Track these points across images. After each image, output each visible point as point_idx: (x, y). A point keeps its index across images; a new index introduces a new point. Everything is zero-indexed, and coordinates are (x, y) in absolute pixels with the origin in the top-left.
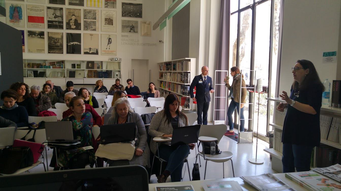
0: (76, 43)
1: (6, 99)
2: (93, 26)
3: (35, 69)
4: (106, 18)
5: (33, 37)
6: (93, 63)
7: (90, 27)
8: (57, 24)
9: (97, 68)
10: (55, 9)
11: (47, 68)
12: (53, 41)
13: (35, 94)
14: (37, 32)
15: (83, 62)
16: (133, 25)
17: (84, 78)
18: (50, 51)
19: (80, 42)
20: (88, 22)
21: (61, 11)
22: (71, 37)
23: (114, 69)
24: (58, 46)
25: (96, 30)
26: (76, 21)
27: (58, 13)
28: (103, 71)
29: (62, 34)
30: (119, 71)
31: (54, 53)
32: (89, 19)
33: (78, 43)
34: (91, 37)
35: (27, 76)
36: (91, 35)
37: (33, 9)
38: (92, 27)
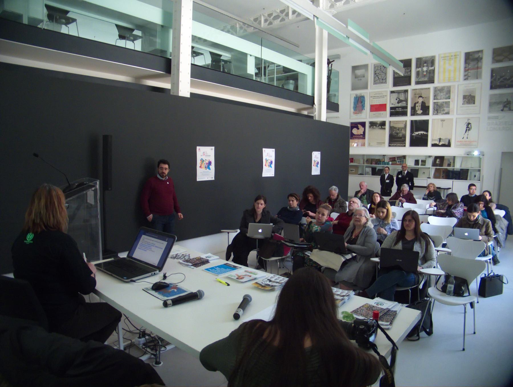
0: (422, 132)
1: (290, 198)
2: (445, 109)
3: (374, 165)
4: (464, 95)
5: (375, 128)
6: (442, 158)
7: (441, 110)
8: (400, 110)
9: (448, 166)
10: (399, 92)
11: (386, 165)
12: (395, 132)
13: (333, 195)
14: (378, 123)
15: (430, 157)
16: (508, 100)
17: (428, 178)
18: (391, 144)
19: (427, 131)
20: (439, 104)
21: (406, 94)
22: (418, 126)
23: (472, 167)
24: (401, 138)
25: (450, 113)
26: (423, 103)
27: (402, 97)
28: (455, 170)
29: (405, 122)
30: (479, 171)
31: (395, 146)
32: (440, 99)
33: (425, 133)
34: (443, 123)
35: (364, 174)
36: (443, 120)
37: (376, 96)
38: (444, 110)
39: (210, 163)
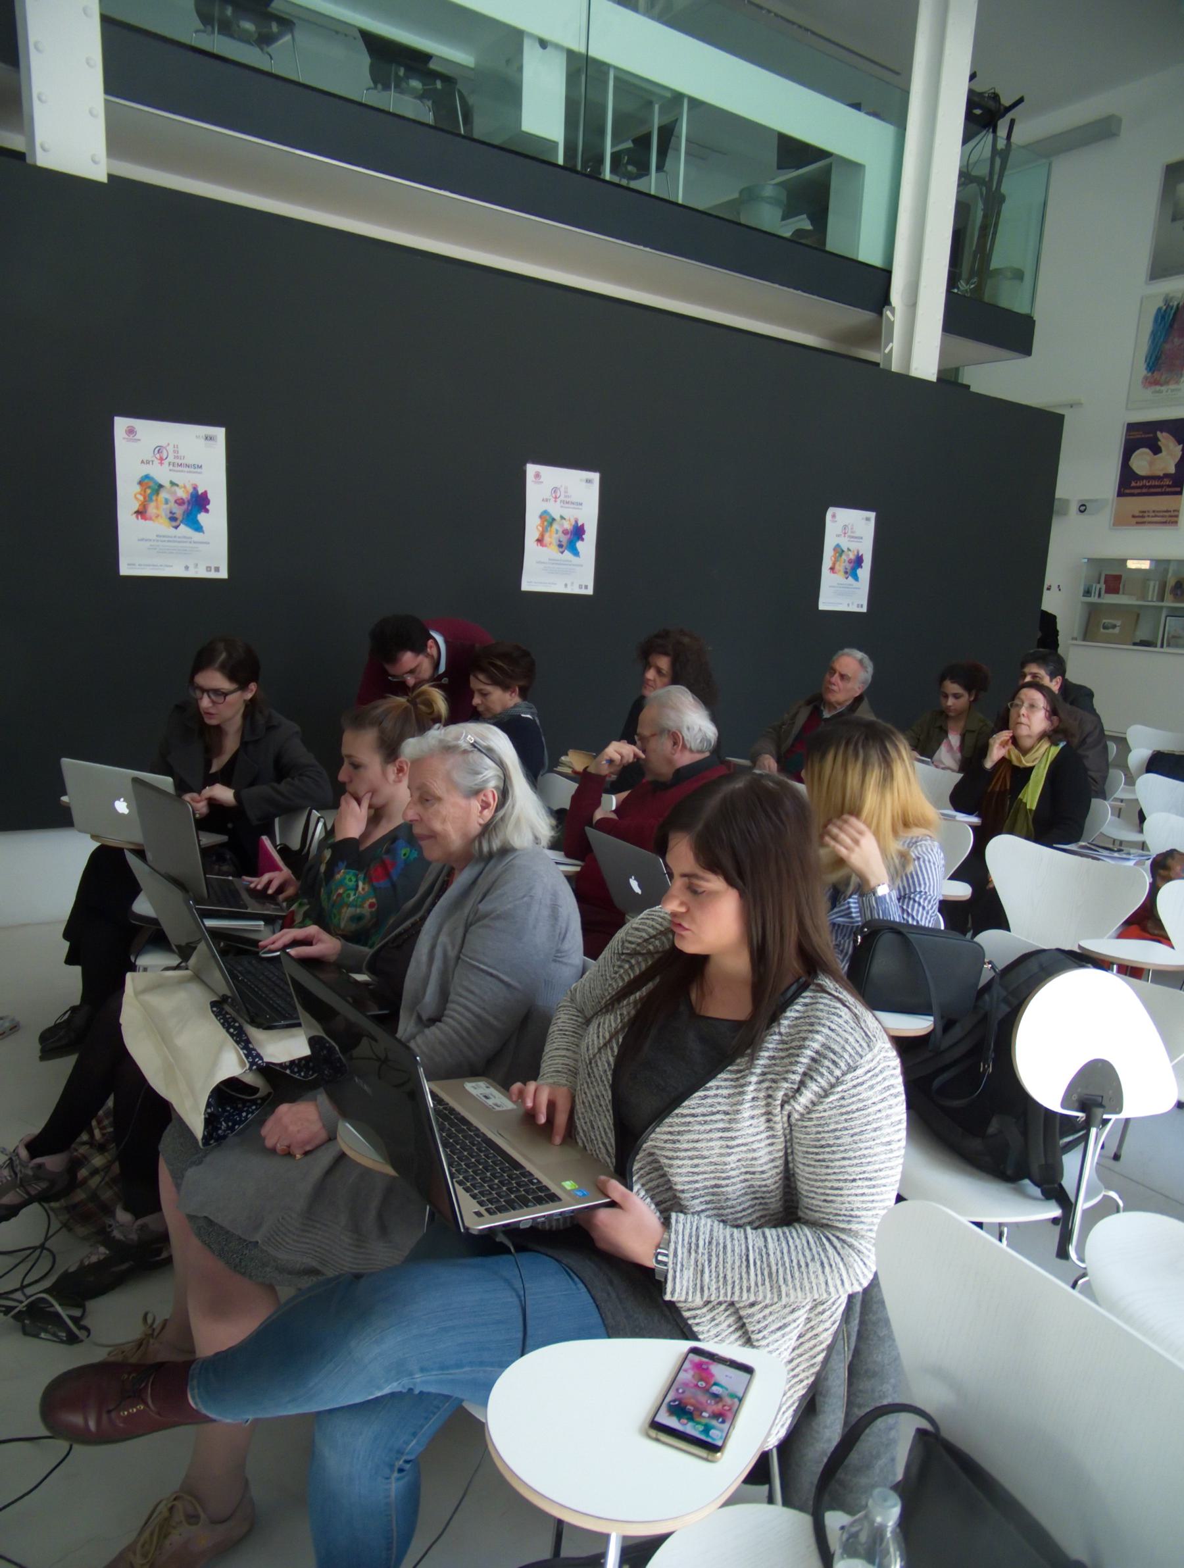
39: (200, 501)
